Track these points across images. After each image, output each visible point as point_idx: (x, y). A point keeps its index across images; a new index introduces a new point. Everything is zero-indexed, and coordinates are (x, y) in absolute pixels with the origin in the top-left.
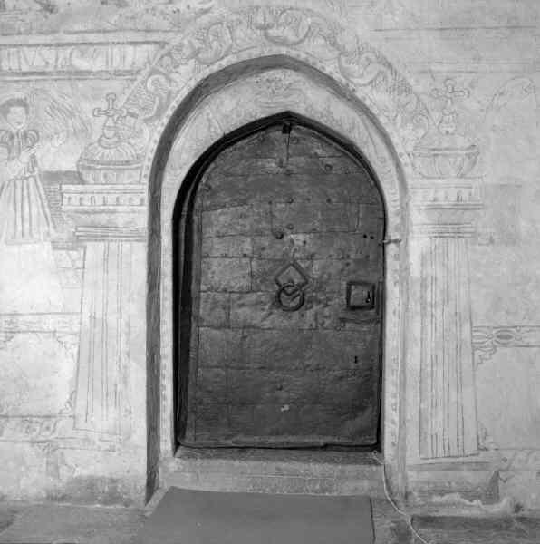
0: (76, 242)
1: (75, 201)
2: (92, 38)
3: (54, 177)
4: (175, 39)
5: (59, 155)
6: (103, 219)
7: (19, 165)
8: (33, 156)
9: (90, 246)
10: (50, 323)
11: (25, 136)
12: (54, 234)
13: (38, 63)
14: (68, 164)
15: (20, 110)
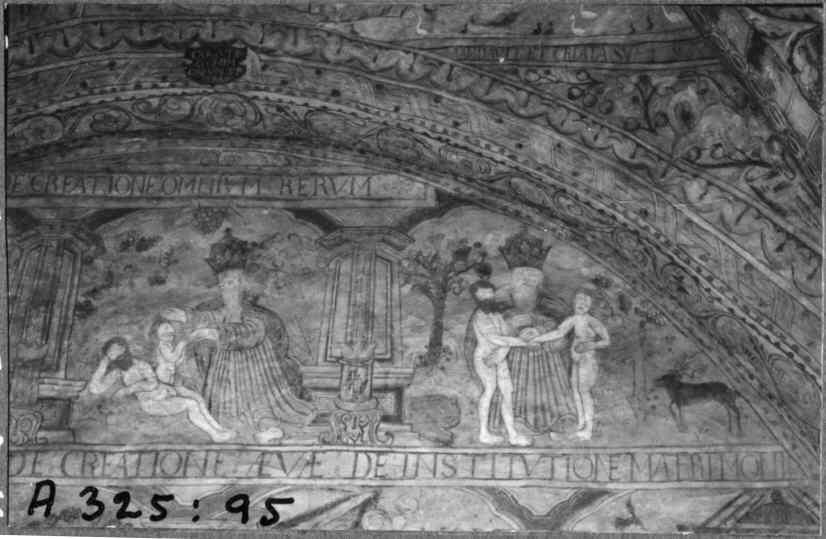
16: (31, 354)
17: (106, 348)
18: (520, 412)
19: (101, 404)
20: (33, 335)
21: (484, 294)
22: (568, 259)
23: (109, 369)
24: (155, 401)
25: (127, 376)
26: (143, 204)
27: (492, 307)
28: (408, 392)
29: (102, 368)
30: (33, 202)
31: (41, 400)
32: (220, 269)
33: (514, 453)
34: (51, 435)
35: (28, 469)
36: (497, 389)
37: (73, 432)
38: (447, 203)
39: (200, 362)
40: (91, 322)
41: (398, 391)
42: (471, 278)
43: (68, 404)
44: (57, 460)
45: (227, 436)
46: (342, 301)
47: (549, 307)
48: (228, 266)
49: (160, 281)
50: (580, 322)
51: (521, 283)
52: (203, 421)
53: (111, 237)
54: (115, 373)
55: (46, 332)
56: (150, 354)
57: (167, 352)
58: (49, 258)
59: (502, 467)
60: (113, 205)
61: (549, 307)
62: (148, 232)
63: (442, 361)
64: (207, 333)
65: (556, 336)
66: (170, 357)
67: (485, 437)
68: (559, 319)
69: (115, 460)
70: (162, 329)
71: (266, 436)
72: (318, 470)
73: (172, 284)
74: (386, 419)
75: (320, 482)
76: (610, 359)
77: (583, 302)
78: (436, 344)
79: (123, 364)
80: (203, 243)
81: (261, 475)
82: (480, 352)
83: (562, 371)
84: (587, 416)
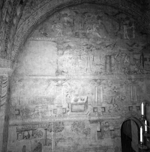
0: (114, 138)
1: (113, 133)
2: (115, 115)
3: (111, 130)
4: (123, 115)
5: (111, 128)
6: (116, 135)
7: (107, 129)
8: (109, 129)
9: (115, 138)
10: (112, 147)
11: (108, 126)
12: (111, 137)
13: (109, 118)
14: (112, 129)
15: (107, 123)
16: (80, 28)
17: (88, 28)
18: (128, 36)
19: (89, 34)
20: (80, 26)
21: (124, 23)
22: (132, 19)
23: (89, 30)
24: (93, 33)
25: (91, 31)
26: (89, 11)
27: (125, 24)
28: (118, 33)
29: (88, 29)
30: (77, 11)
31: (82, 33)
32: (98, 19)
33: (127, 39)
34: (84, 37)
35: (83, 40)
36: (126, 34)
37: (86, 36)
38: (119, 13)
39: (97, 30)
40: (86, 25)
41: (117, 33)
42: (123, 21)
43: (85, 33)
44: (85, 39)
45: (101, 37)
46: (111, 23)
47: (130, 25)
48: (99, 19)
49: (92, 21)
50: (133, 26)
51: (127, 22)
52: (99, 36)
53: (86, 15)
54: (89, 30)
55: (81, 25)
56: (93, 28)
57: (94, 28)
58: (80, 17)
59: (127, 41)
60: (86, 11)
61: (130, 25)
62: (90, 15)
63: (121, 30)
64: (98, 26)
65: (131, 28)
66: (94, 29)
67: (125, 38)
68: (131, 26)
69: (91, 39)
70: (93, 26)
71: (105, 37)
72: (110, 41)
73: (93, 21)
74: (116, 36)
75: (110, 42)
76: (136, 30)
77: (133, 24)
78: (120, 28)
79: (90, 29)
80: (96, 16)
81: (105, 41)
82: (124, 29)
83: (131, 31)
84: (134, 36)
